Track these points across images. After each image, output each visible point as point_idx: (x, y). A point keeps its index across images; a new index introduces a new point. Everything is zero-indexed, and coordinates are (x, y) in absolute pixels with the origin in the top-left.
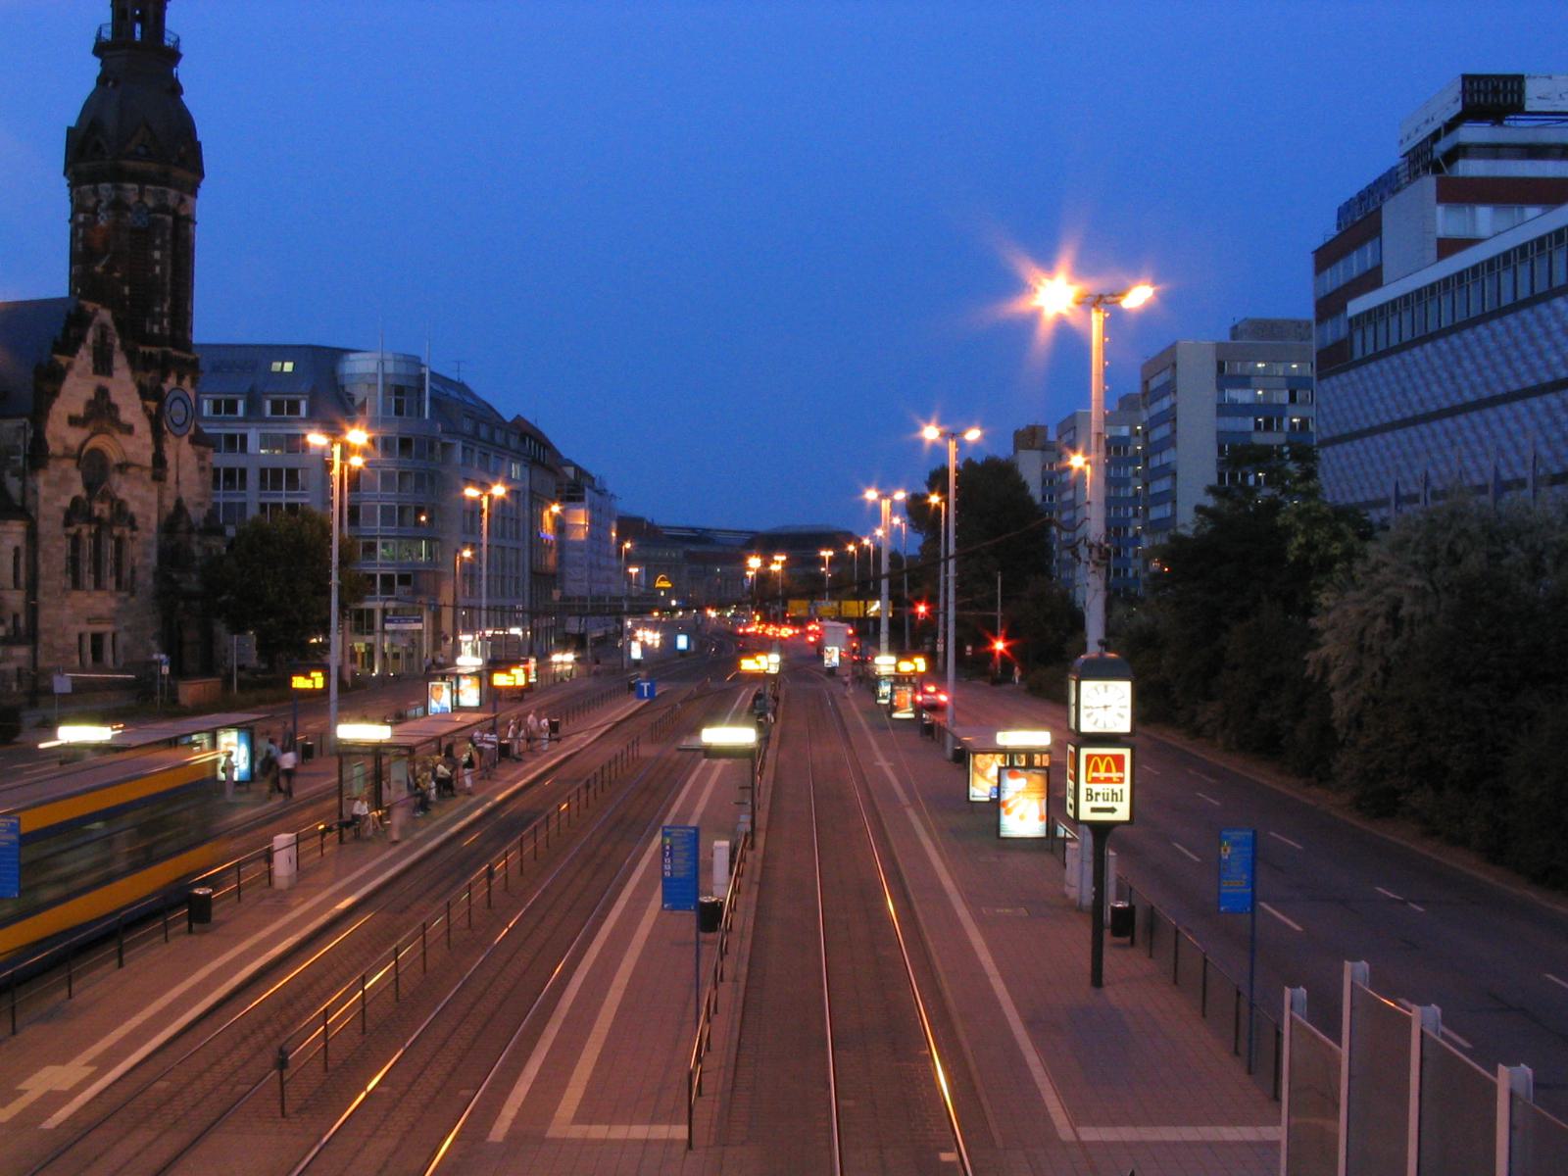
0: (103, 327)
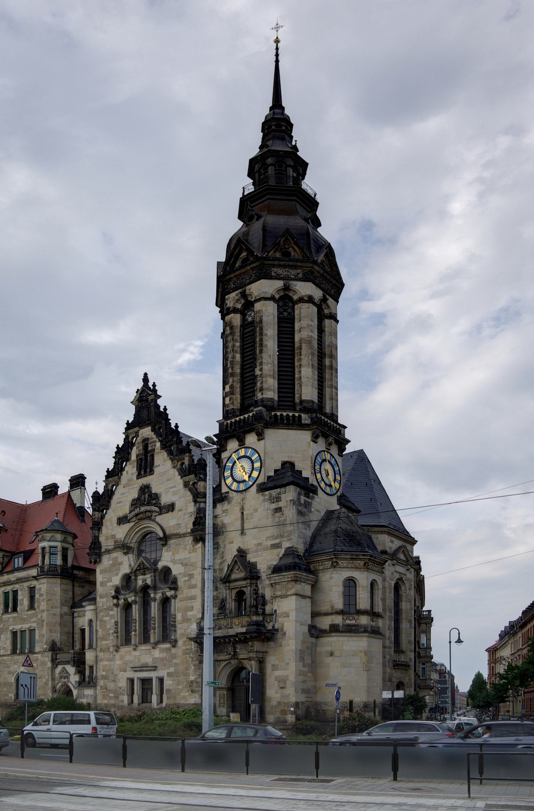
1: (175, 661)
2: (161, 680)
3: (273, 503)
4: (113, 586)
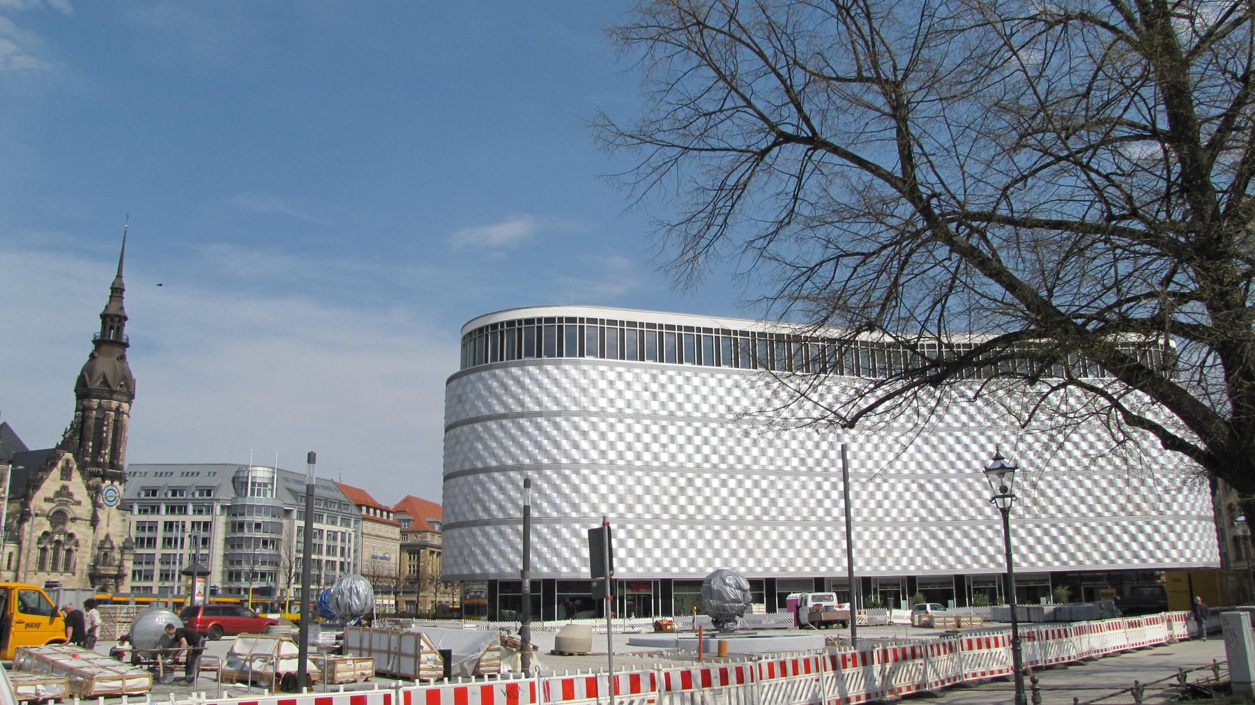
0: (68, 461)
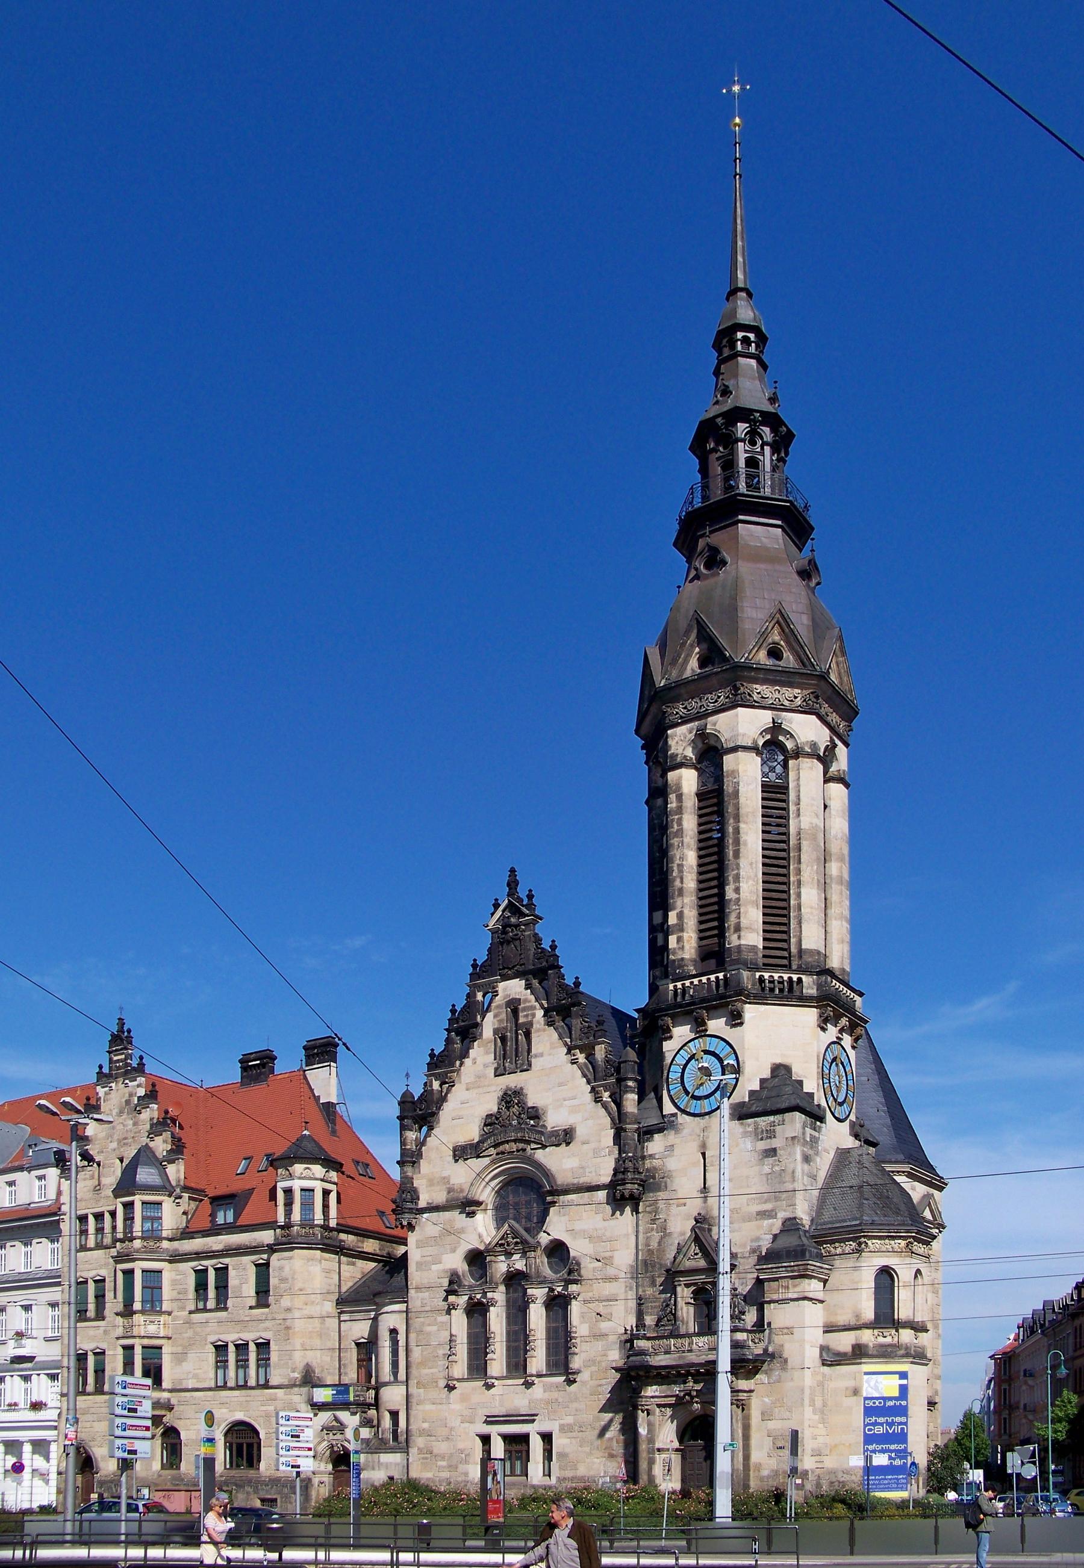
0: (514, 1006)
1: (575, 1405)
2: (547, 1438)
3: (762, 1139)
4: (445, 1271)
